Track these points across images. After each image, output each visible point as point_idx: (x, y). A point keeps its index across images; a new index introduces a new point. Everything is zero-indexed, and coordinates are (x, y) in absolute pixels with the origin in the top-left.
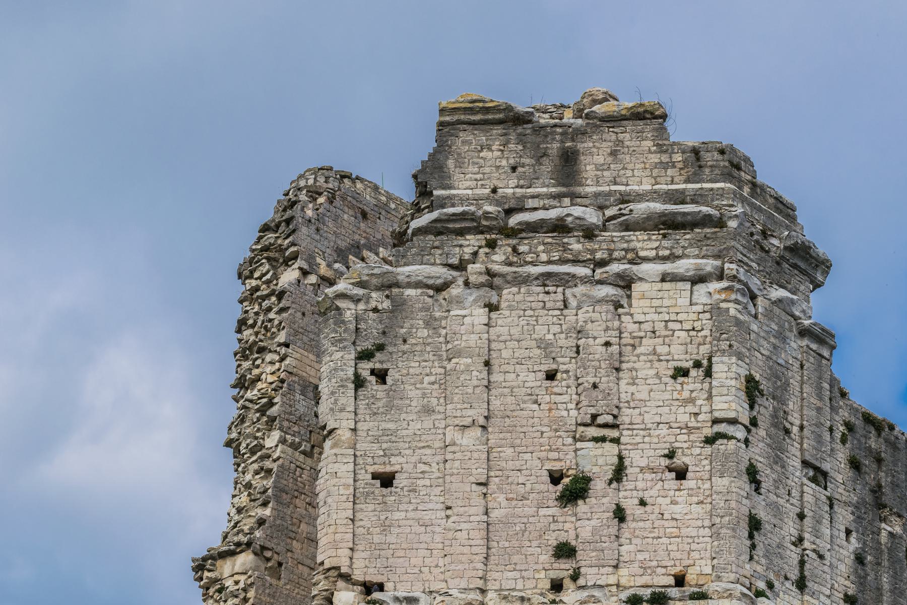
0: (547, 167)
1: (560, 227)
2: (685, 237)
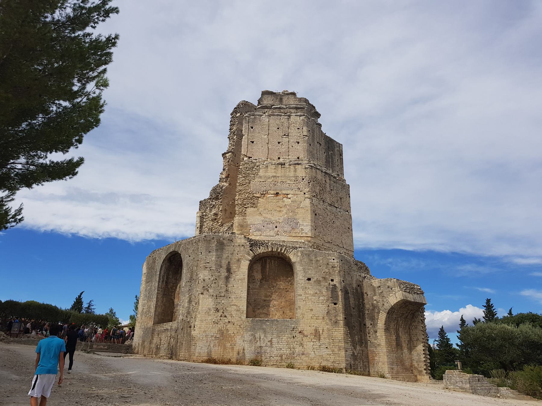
0: (278, 100)
1: (280, 108)
2: (299, 110)
